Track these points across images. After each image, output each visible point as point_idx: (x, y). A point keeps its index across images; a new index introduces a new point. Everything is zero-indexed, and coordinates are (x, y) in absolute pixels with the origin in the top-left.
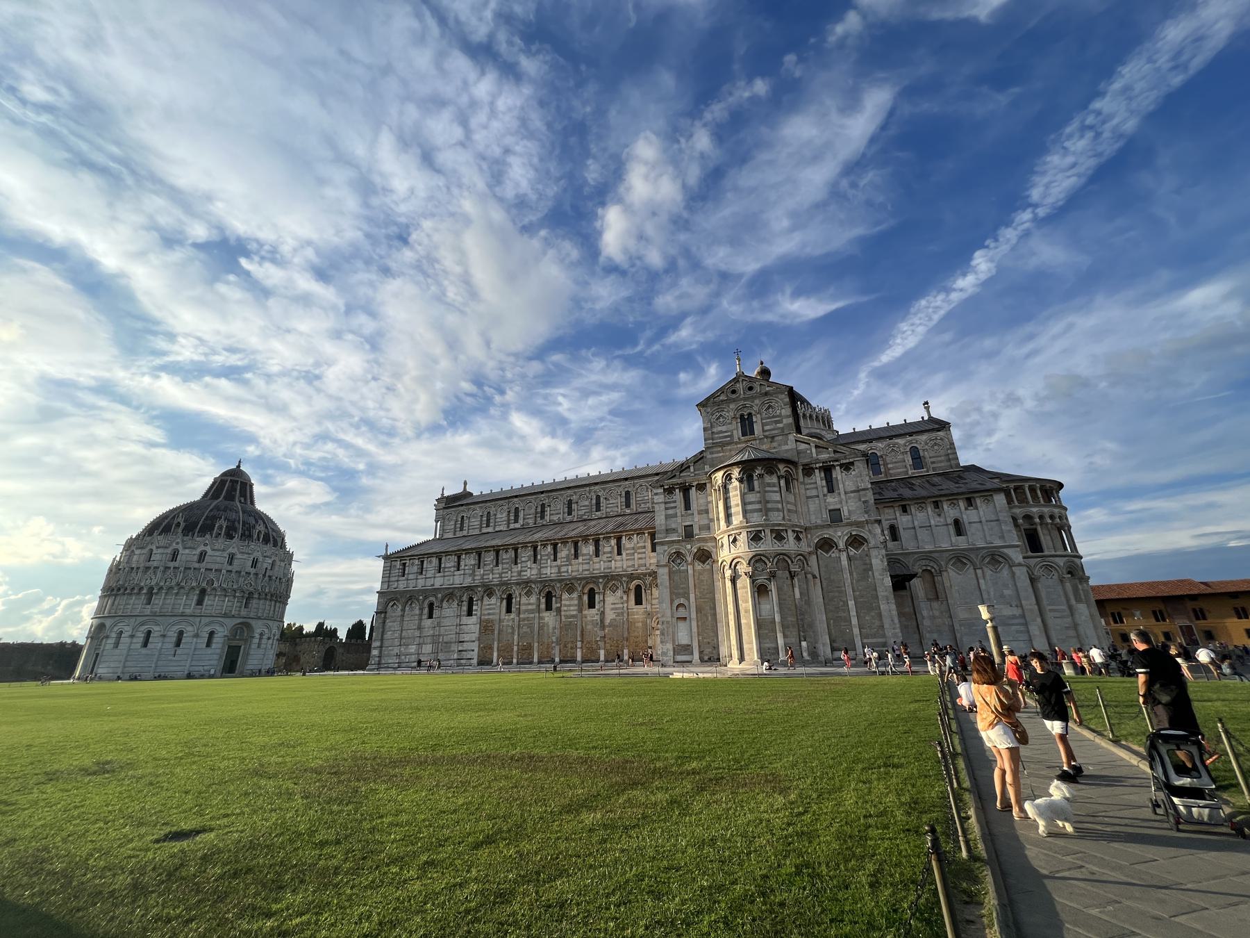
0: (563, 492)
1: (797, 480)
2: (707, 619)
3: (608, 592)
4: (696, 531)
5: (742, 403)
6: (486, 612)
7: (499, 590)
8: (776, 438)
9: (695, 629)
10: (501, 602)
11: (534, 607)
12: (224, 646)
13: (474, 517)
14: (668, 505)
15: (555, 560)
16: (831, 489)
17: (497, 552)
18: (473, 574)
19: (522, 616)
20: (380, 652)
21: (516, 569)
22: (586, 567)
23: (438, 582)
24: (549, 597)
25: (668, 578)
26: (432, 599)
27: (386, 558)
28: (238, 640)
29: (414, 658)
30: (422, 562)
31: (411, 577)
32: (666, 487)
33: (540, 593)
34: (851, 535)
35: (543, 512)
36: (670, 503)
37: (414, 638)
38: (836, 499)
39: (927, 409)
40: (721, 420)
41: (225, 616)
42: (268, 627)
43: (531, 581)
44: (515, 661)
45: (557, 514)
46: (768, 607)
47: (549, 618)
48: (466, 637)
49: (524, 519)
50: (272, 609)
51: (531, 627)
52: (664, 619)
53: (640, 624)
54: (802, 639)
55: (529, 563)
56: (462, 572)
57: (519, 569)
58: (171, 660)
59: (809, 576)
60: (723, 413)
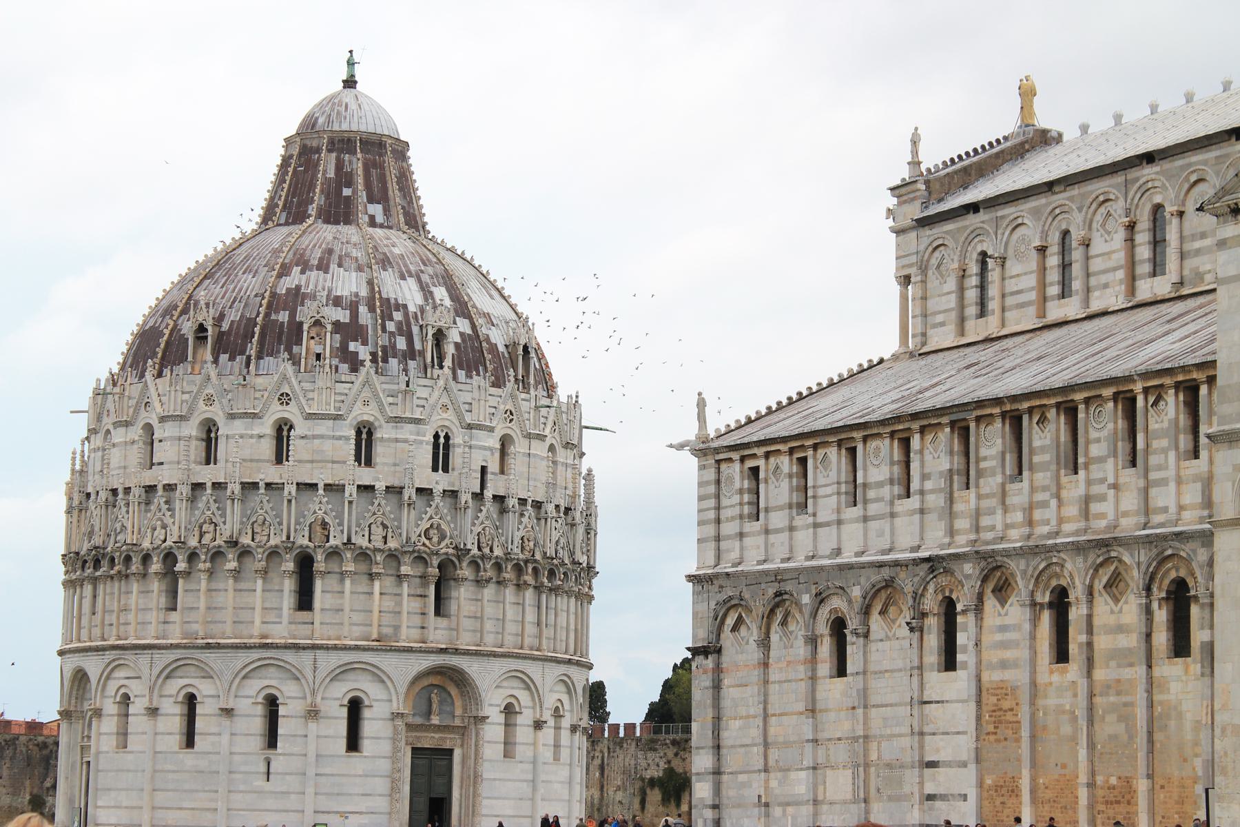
7: (1024, 572)
10: (1035, 621)
12: (396, 750)
13: (1019, 256)
19: (1099, 674)
21: (1075, 487)
27: (706, 450)
28: (439, 728)
30: (803, 461)
33: (1148, 589)
41: (384, 645)
42: (528, 684)
48: (938, 749)
49: (1183, 256)
50: (531, 616)
55: (1110, 464)
58: (260, 792)
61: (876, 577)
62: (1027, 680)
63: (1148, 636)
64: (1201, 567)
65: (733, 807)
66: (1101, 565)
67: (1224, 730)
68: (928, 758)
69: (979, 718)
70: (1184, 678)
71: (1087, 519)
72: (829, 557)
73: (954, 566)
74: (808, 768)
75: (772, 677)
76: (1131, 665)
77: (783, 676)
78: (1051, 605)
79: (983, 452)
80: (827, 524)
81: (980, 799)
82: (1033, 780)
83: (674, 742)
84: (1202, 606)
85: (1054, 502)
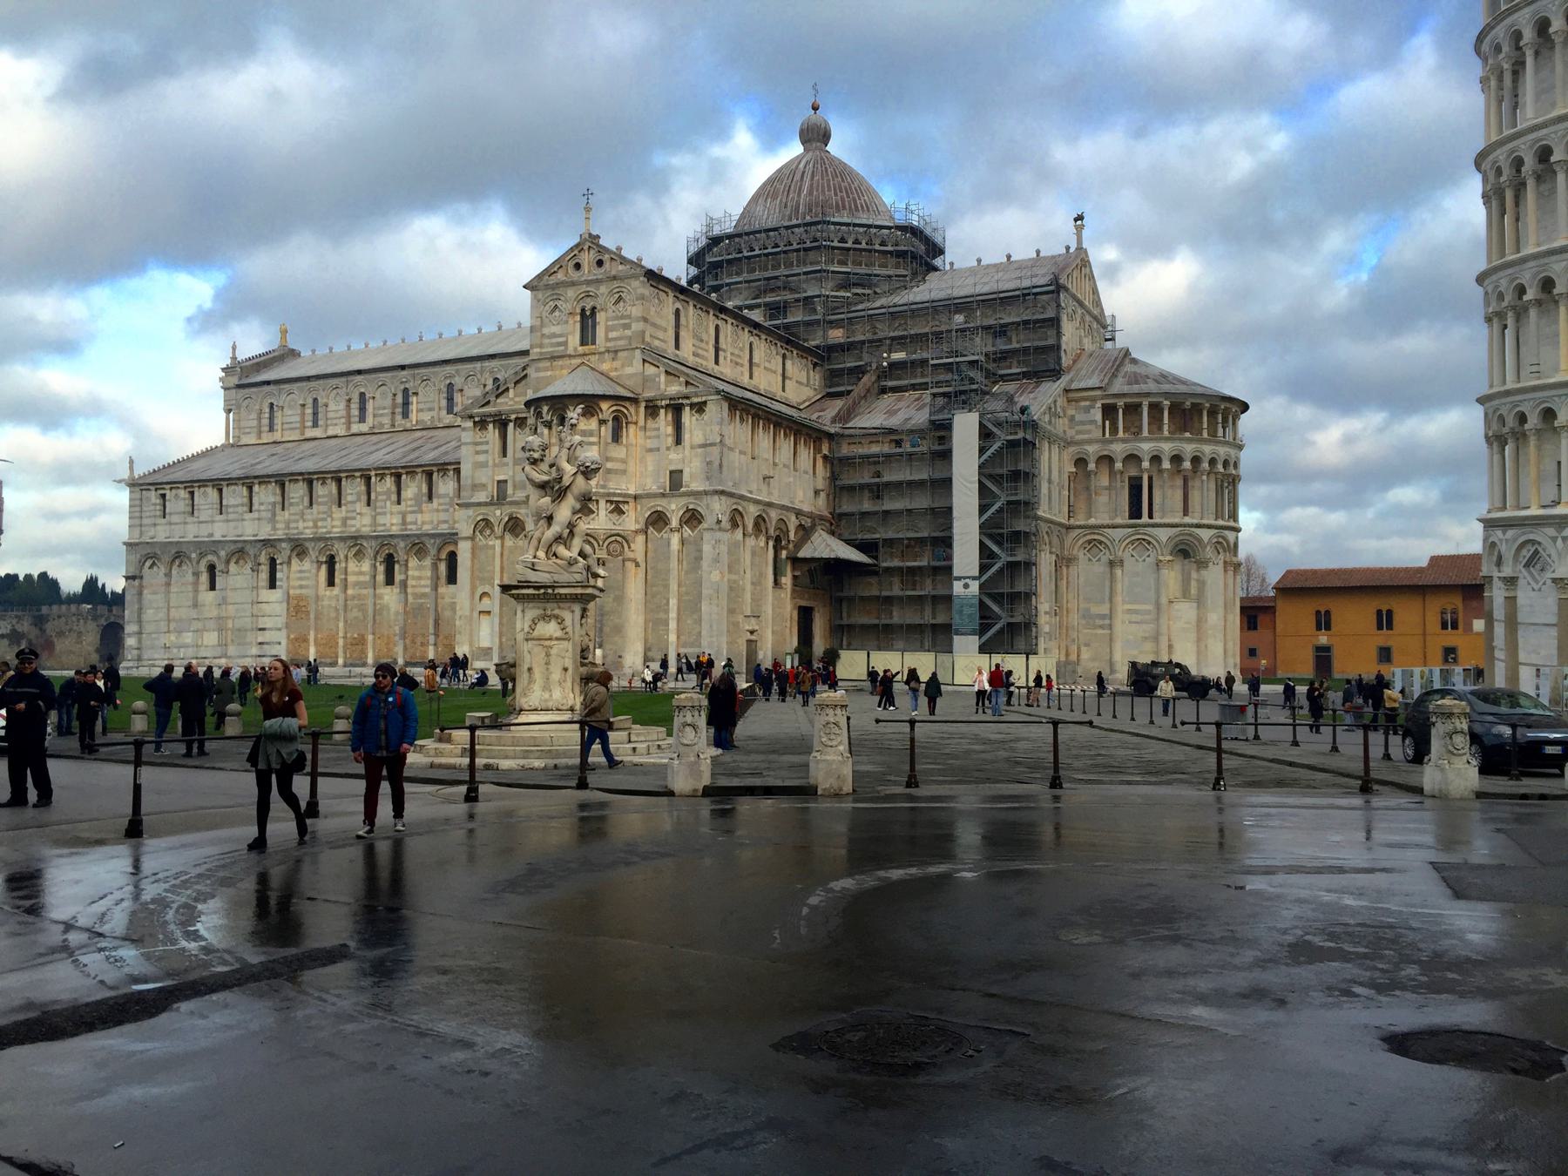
0: (437, 369)
1: (636, 423)
4: (510, 491)
5: (584, 288)
7: (313, 549)
8: (620, 354)
11: (367, 578)
13: (290, 407)
14: (479, 448)
15: (399, 503)
16: (678, 440)
17: (310, 483)
18: (273, 520)
19: (350, 592)
20: (140, 641)
21: (339, 514)
22: (443, 516)
23: (220, 530)
24: (390, 562)
26: (210, 557)
30: (192, 493)
31: (175, 519)
32: (477, 419)
34: (688, 510)
35: (406, 404)
36: (481, 443)
38: (681, 456)
39: (1079, 229)
40: (557, 313)
43: (362, 537)
44: (341, 661)
45: (430, 409)
47: (390, 596)
49: (374, 416)
51: (362, 608)
55: (358, 505)
60: (559, 303)
61: (233, 547)
63: (375, 577)
69: (288, 610)
73: (278, 544)
78: (326, 562)
79: (292, 495)
80: (206, 522)
81: (288, 644)
83: (16, 617)
84: (401, 566)
85: (329, 519)
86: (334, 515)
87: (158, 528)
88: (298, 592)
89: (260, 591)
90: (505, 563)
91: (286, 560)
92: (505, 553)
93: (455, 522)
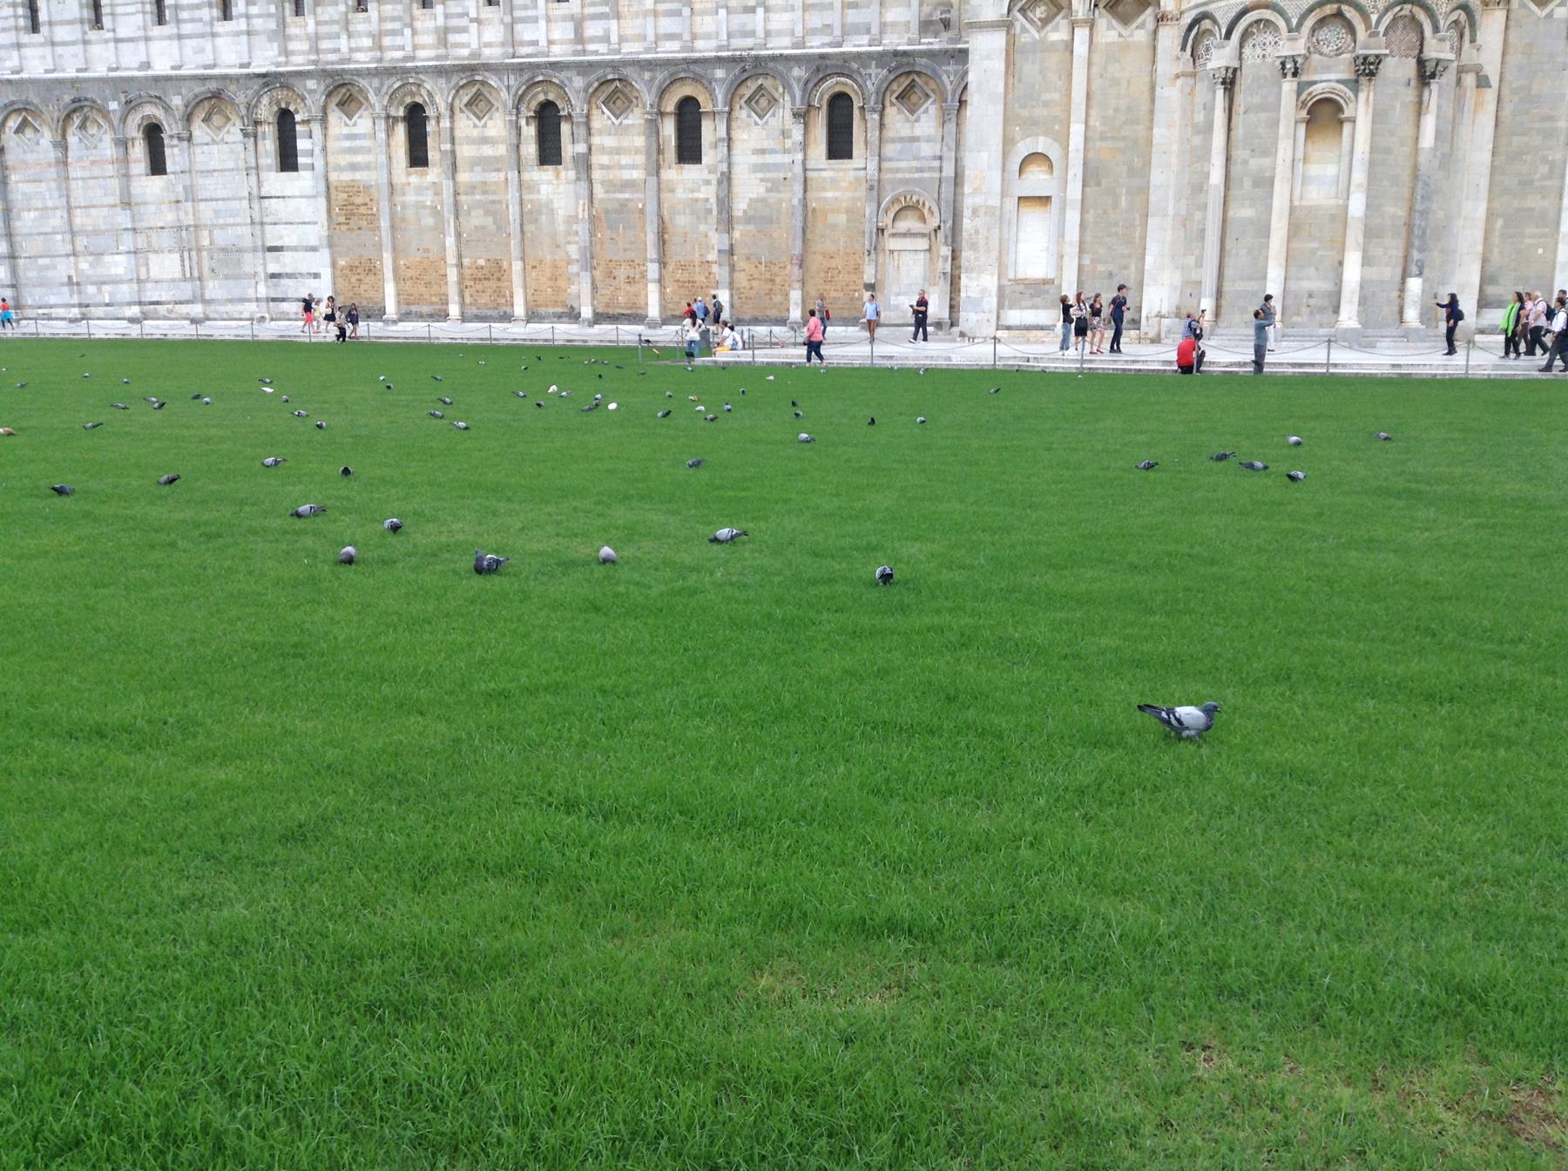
2: (1116, 205)
3: (742, 114)
6: (344, 160)
7: (378, 91)
9: (1073, 234)
10: (389, 132)
11: (502, 150)
19: (464, 177)
22: (667, 25)
24: (548, 120)
25: (1002, 67)
26: (149, 110)
29: (126, 291)
31: (62, 33)
37: (117, 233)
43: (487, 67)
44: (454, 310)
46: (1331, 170)
51: (494, 210)
52: (979, 200)
53: (842, 219)
54: (1414, 269)
56: (242, 25)
57: (440, 21)
59: (1469, 80)
61: (199, 89)
62: (386, 181)
64: (578, 92)
65: (34, 286)
66: (462, 87)
67: (975, 212)
68: (269, 244)
69: (329, 211)
70: (555, 182)
71: (446, 47)
72: (139, 69)
73: (298, 86)
74: (128, 252)
75: (72, 174)
76: (498, 170)
77: (87, 174)
80: (131, 40)
82: (394, 261)
85: (408, 32)
86: (418, 24)
87: (27, 52)
88: (346, 176)
89: (263, 175)
90: (1096, 85)
91: (316, 111)
92: (1096, 58)
93: (694, 37)
